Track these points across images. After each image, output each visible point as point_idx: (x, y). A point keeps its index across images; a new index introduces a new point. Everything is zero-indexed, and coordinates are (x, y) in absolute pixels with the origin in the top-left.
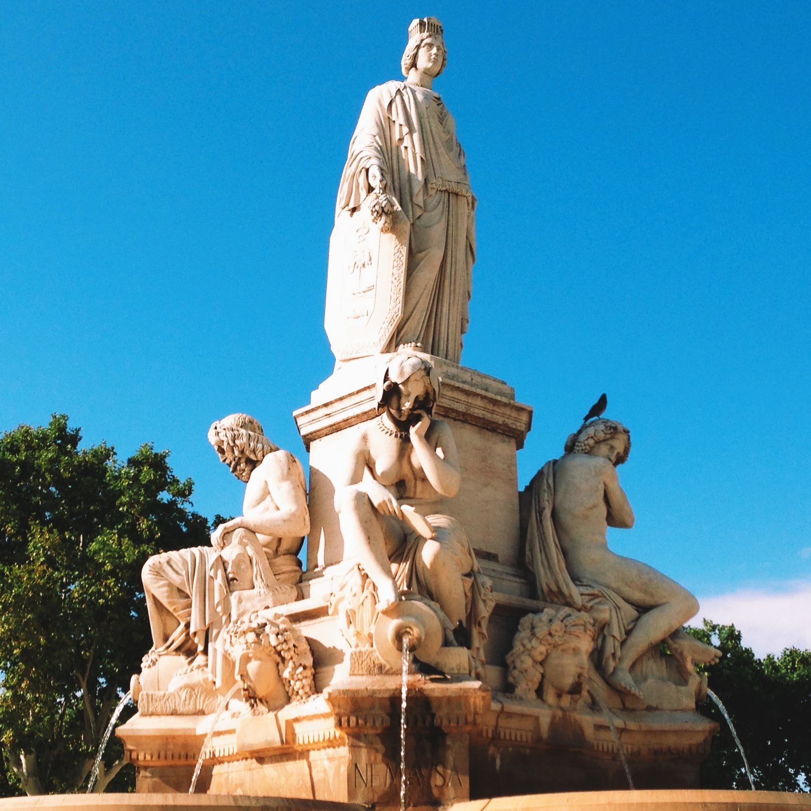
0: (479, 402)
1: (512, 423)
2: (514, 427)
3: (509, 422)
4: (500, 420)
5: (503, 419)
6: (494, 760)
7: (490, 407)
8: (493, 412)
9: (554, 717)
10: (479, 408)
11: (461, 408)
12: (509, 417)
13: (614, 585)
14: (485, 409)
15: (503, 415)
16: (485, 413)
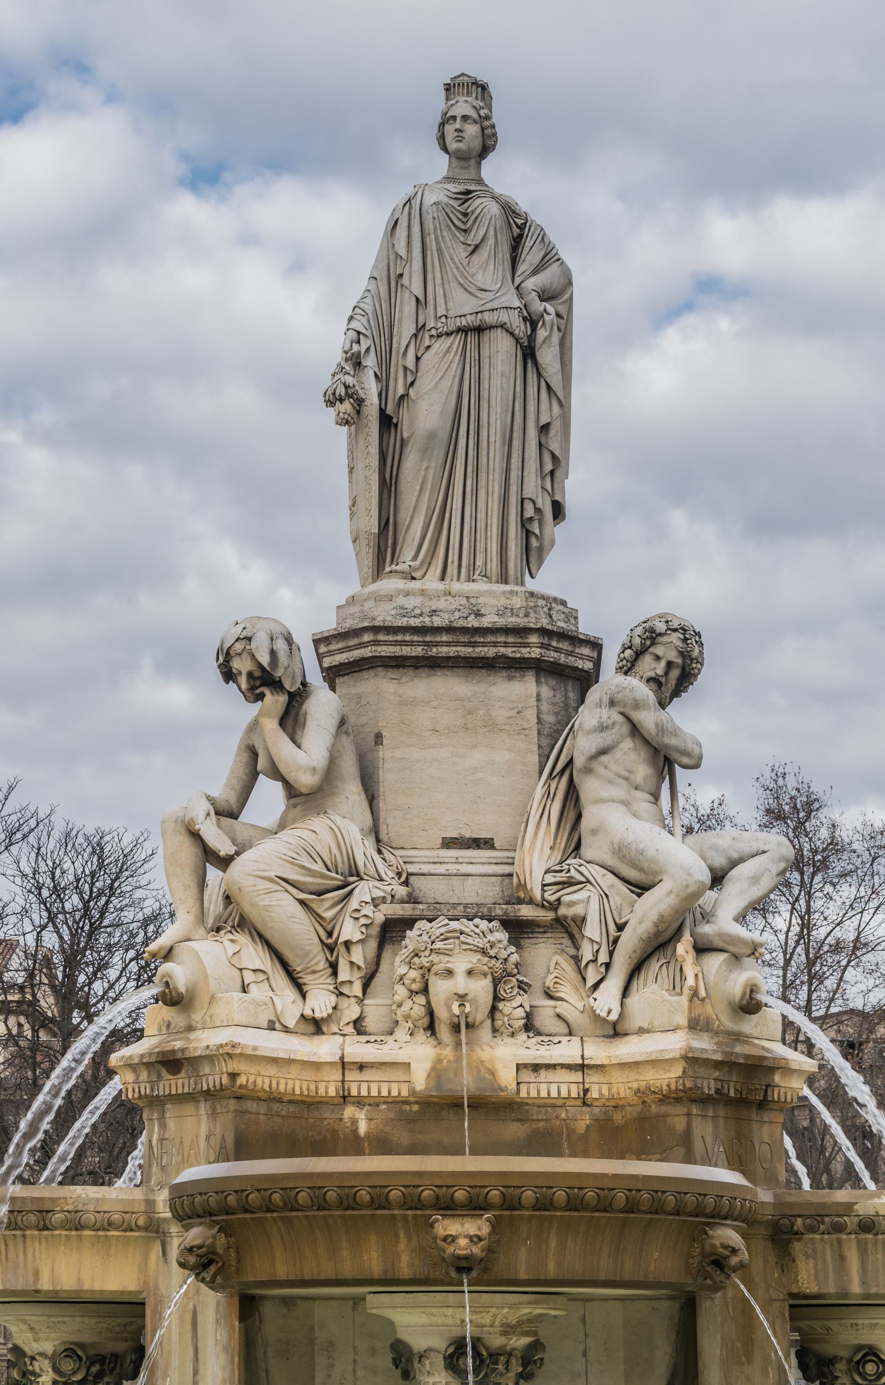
0: (445, 638)
1: (513, 652)
2: (518, 655)
3: (508, 651)
4: (490, 652)
5: (495, 650)
6: (354, 1122)
7: (465, 639)
8: (474, 644)
9: (439, 1061)
10: (448, 644)
11: (418, 651)
12: (506, 644)
13: (610, 863)
14: (456, 643)
15: (495, 644)
16: (459, 648)
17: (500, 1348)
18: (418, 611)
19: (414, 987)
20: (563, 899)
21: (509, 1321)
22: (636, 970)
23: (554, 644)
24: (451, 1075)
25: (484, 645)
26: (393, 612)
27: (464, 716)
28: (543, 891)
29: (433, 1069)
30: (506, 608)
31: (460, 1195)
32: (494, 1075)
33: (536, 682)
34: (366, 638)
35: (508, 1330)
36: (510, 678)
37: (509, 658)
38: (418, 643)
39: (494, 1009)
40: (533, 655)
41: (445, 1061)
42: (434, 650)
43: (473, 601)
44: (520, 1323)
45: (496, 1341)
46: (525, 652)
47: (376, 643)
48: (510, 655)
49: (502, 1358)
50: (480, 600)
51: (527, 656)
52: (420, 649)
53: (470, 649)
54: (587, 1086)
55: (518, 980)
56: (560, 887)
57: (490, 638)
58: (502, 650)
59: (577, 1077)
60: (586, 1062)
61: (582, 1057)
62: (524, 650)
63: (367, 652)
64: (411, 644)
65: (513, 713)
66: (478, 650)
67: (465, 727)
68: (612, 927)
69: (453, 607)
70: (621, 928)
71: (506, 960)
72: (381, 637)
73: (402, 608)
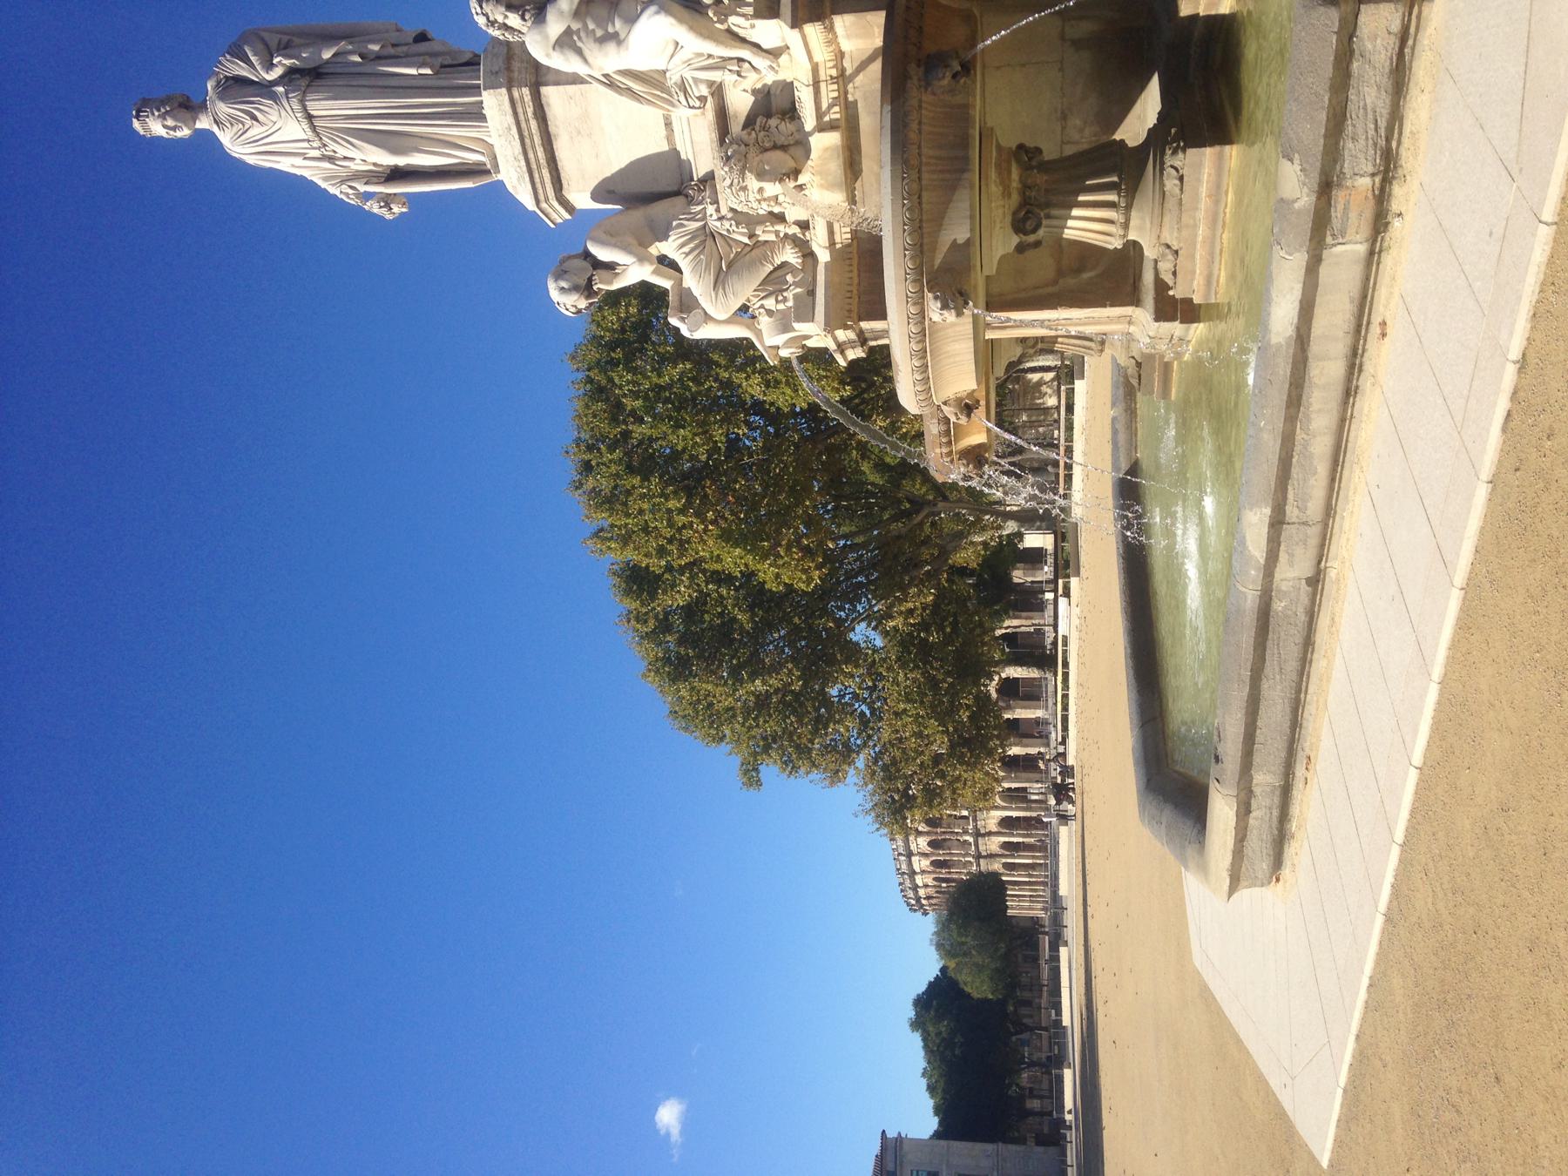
0: (531, 156)
2: (531, 104)
3: (530, 111)
4: (534, 124)
8: (531, 135)
9: (822, 186)
10: (535, 153)
12: (525, 113)
15: (527, 121)
17: (1019, 194)
18: (518, 169)
19: (772, 203)
20: (697, 95)
21: (1000, 193)
22: (743, 41)
23: (516, 74)
24: (830, 178)
25: (529, 129)
26: (523, 184)
27: (582, 136)
28: (693, 107)
29: (828, 189)
30: (500, 109)
31: (913, 310)
32: (827, 149)
33: (546, 85)
34: (544, 205)
35: (1007, 193)
36: (549, 105)
37: (534, 110)
38: (540, 173)
39: (784, 148)
40: (528, 92)
41: (823, 182)
42: (541, 161)
43: (501, 132)
44: (1002, 183)
45: (1015, 198)
46: (528, 98)
47: (547, 200)
48: (532, 109)
49: (1027, 193)
50: (500, 128)
51: (529, 97)
52: (543, 171)
53: (535, 137)
54: (829, 78)
55: (760, 131)
56: (688, 96)
57: (523, 125)
58: (530, 114)
59: (823, 86)
60: (811, 83)
61: (808, 86)
62: (526, 100)
63: (556, 204)
64: (541, 177)
65: (572, 101)
66: (534, 131)
67: (590, 135)
68: (711, 61)
69: (509, 146)
70: (710, 56)
71: (746, 145)
72: (542, 197)
73: (518, 180)
